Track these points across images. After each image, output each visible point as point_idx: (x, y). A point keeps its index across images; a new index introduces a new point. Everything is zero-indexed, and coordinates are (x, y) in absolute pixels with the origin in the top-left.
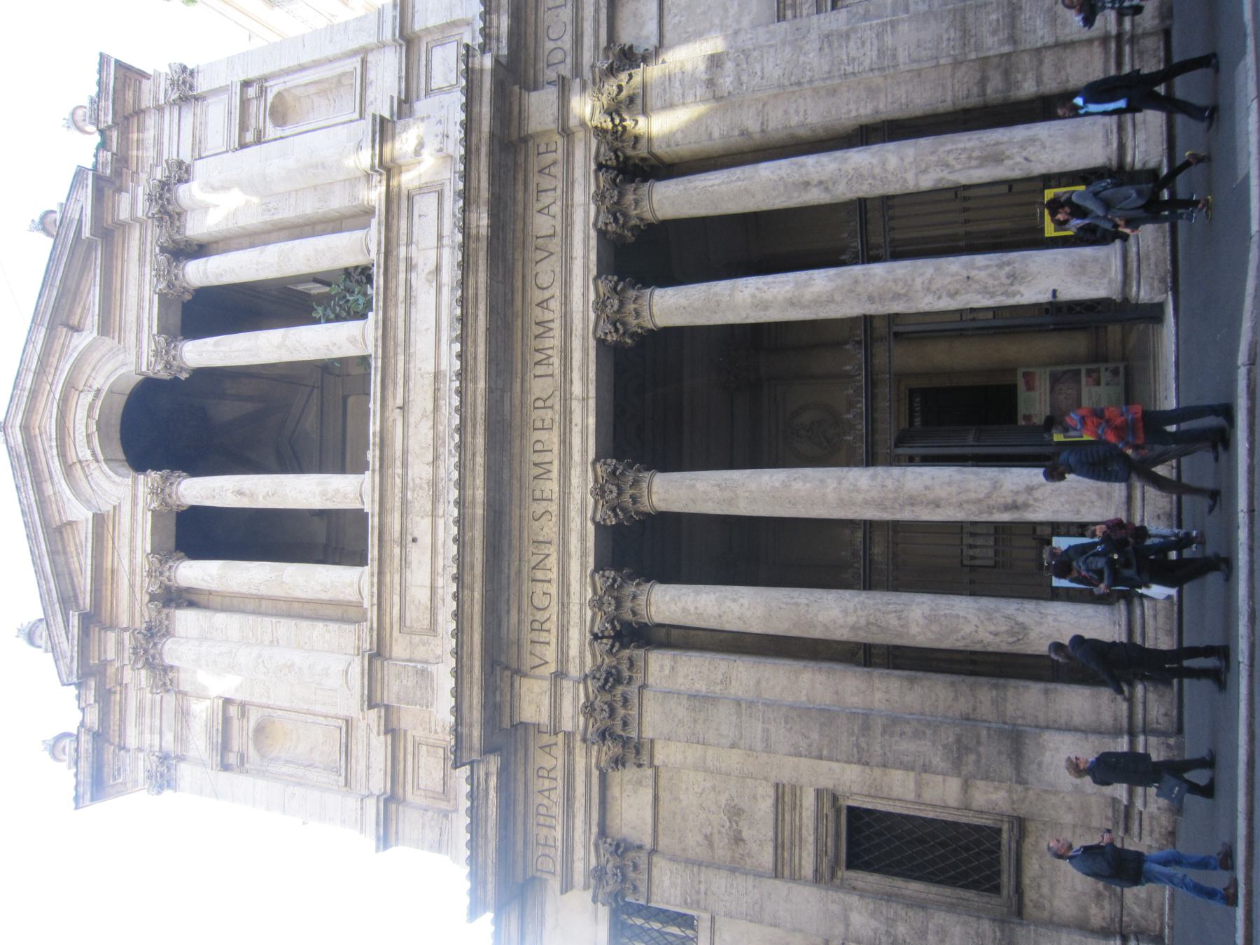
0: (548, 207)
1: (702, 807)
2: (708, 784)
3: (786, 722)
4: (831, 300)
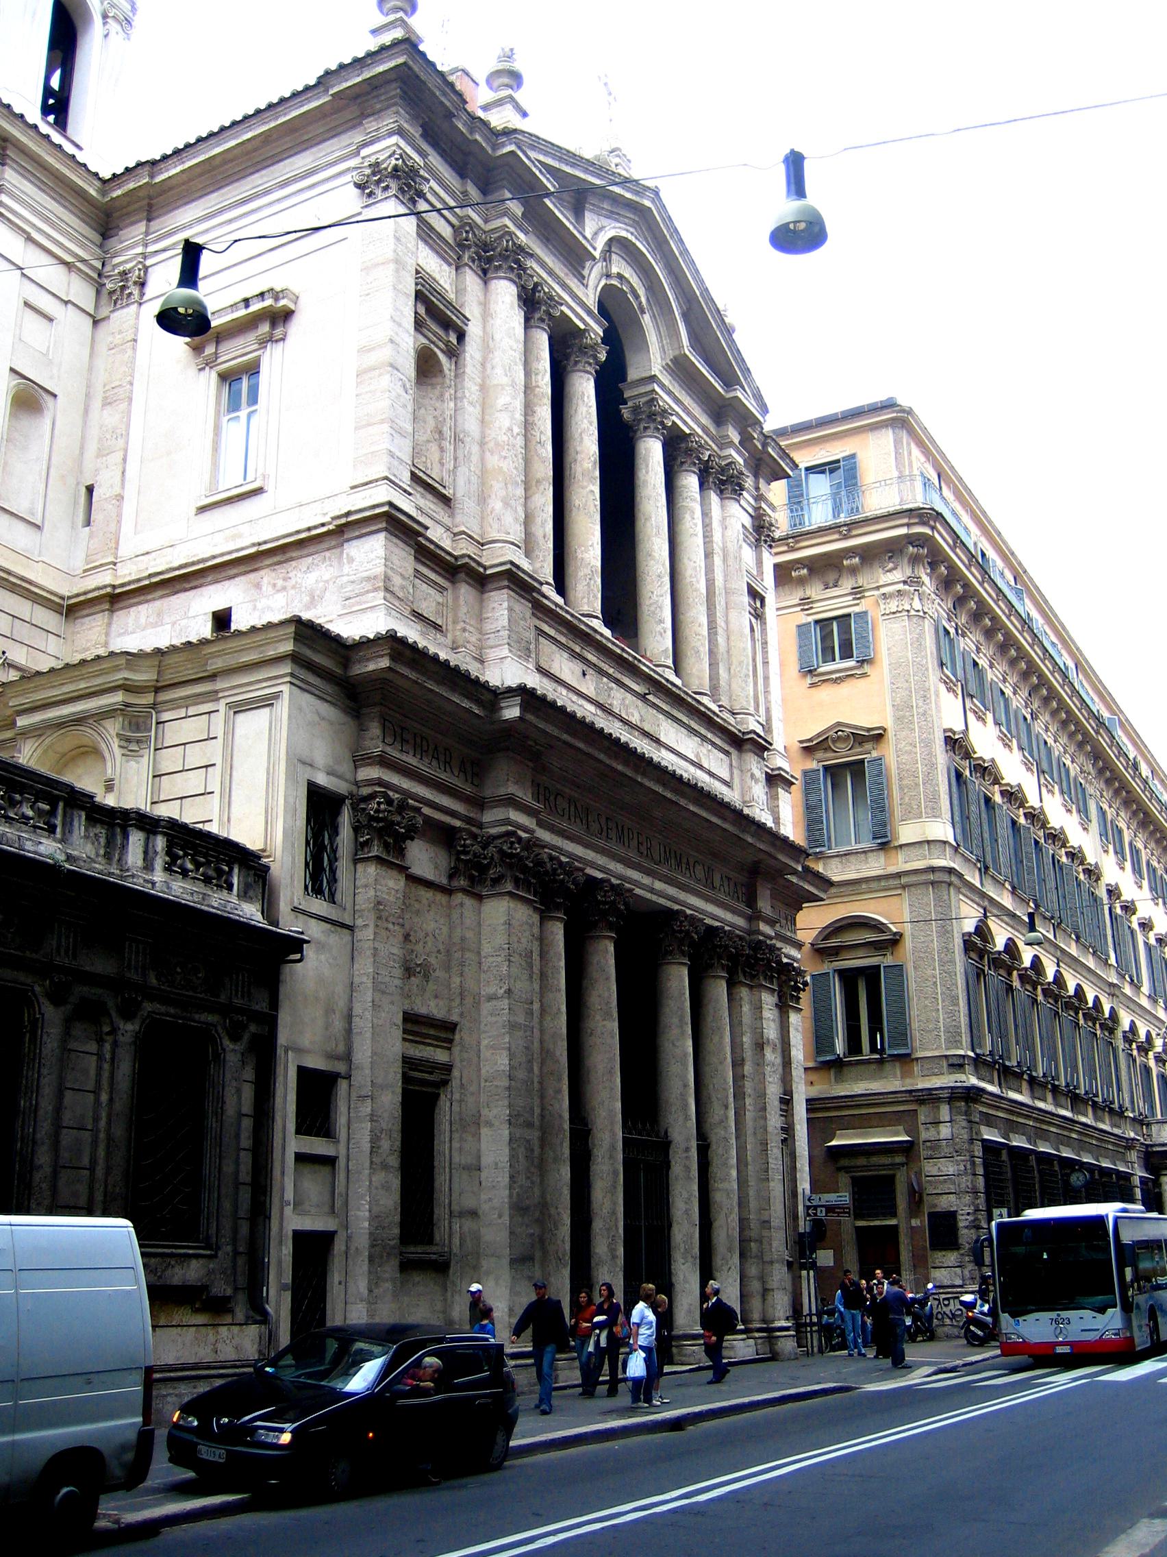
2: (441, 947)
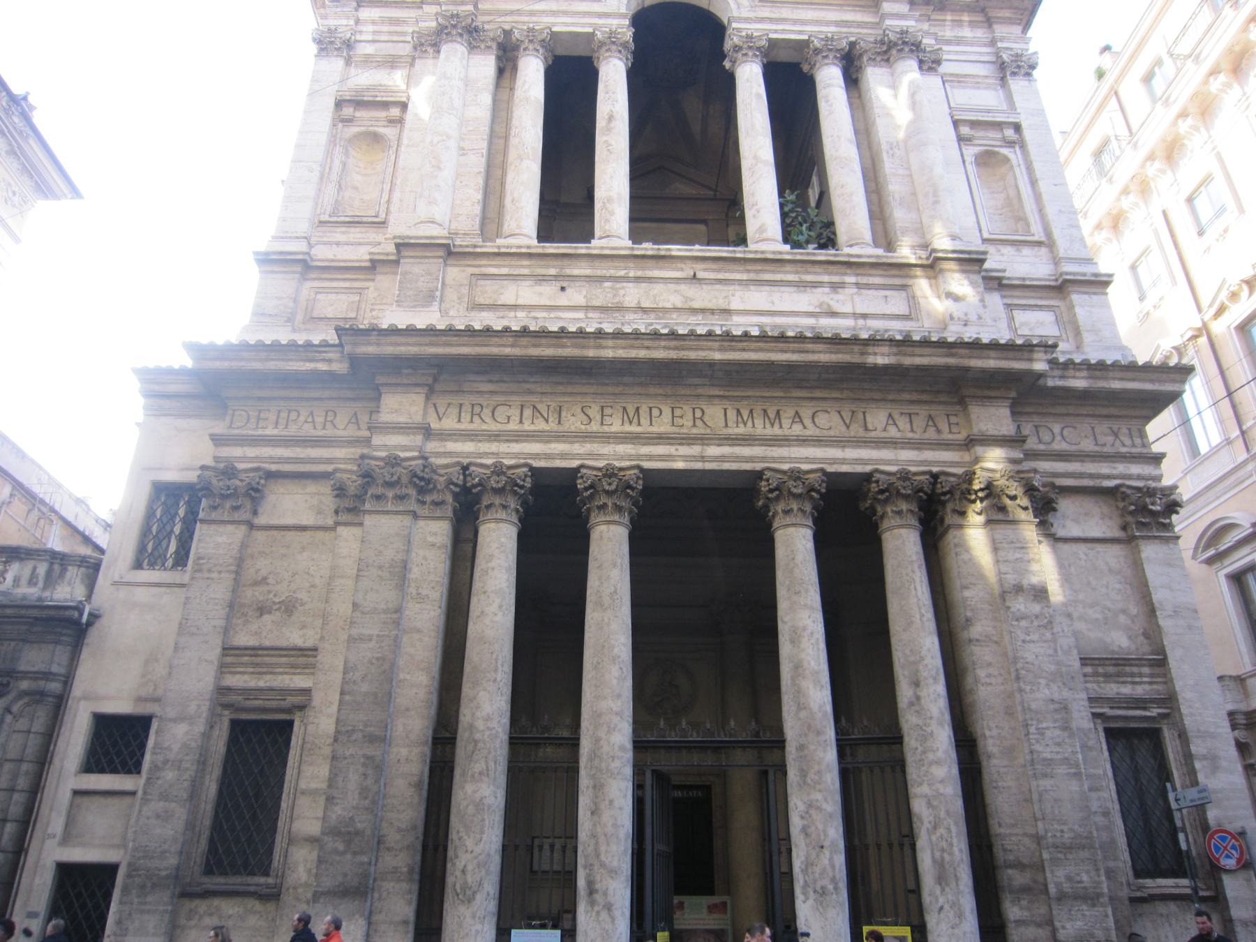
0: (895, 424)
1: (294, 575)
2: (317, 581)
3: (378, 659)
4: (800, 707)
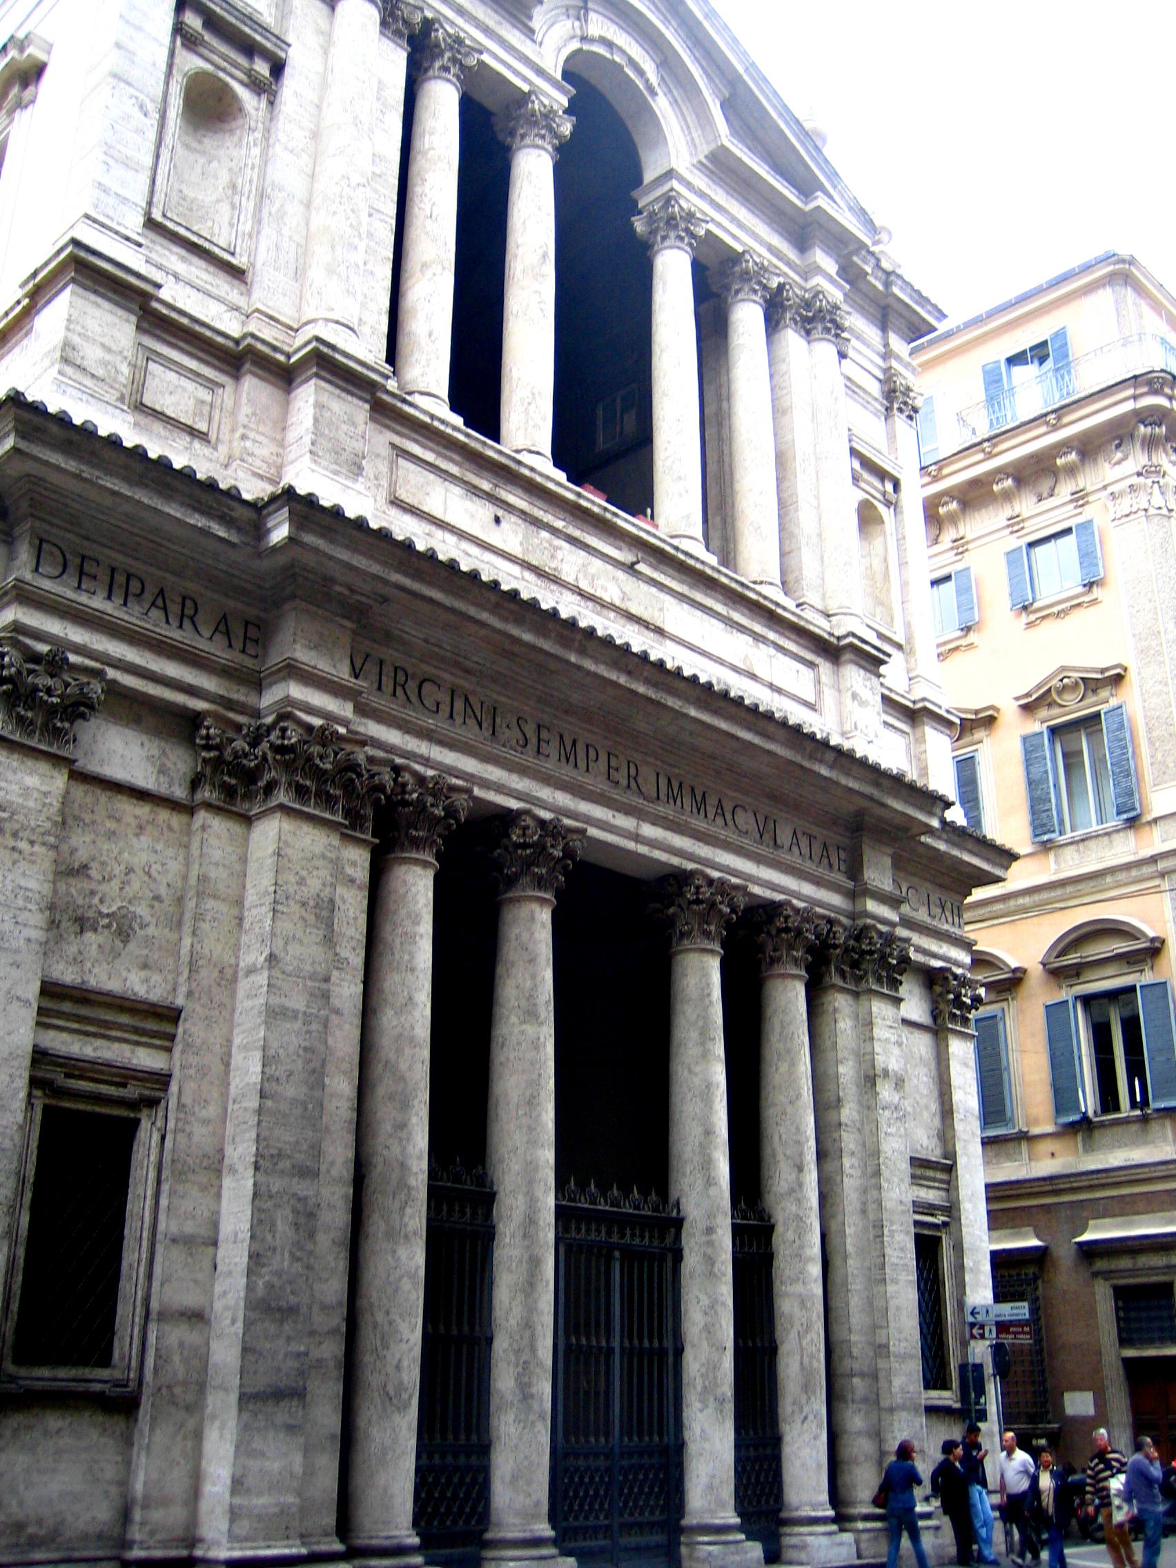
1: (130, 870)
2: (163, 891)
3: (305, 1049)
